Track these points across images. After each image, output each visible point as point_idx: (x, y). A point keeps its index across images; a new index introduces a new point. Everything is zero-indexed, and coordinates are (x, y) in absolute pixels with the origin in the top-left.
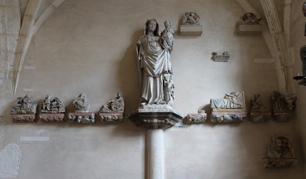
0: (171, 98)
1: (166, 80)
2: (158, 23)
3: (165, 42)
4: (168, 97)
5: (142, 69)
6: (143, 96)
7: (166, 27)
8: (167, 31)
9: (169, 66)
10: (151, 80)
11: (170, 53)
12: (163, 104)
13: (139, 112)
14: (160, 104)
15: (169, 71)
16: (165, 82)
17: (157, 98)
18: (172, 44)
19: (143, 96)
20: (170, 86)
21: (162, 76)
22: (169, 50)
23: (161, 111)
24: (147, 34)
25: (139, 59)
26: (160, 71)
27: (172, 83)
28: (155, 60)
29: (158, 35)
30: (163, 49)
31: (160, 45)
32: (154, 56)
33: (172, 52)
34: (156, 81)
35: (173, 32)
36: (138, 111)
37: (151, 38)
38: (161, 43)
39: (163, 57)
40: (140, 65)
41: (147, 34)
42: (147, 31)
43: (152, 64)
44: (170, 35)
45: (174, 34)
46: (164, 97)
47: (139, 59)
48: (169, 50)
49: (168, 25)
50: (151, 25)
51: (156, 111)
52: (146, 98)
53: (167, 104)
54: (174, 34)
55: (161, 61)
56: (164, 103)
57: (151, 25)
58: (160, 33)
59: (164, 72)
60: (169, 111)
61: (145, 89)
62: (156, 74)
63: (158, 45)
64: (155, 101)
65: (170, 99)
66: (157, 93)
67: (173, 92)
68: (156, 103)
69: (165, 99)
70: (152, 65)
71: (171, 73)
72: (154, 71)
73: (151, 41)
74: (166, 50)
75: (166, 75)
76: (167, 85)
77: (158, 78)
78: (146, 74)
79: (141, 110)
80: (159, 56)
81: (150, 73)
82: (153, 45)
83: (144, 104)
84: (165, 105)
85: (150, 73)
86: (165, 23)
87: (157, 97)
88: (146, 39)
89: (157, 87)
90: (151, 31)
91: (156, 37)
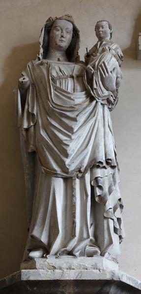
0: (115, 238)
1: (100, 187)
2: (78, 27)
3: (97, 79)
4: (106, 235)
5: (34, 156)
6: (36, 233)
7: (101, 39)
8: (104, 50)
9: (108, 145)
10: (59, 185)
11: (110, 109)
12: (91, 255)
13: (24, 278)
14: (83, 254)
15: (108, 161)
16: (98, 192)
17: (76, 238)
18: (117, 84)
19: (36, 233)
20: (110, 203)
21: (88, 176)
22: (109, 101)
23: (83, 278)
24: (46, 55)
25: (25, 126)
26: (82, 162)
27: (117, 194)
28: (70, 129)
30: (92, 98)
31: (84, 89)
34: (73, 189)
35: (120, 53)
36: (20, 275)
37: (59, 67)
38: (86, 81)
39: (92, 121)
40: (27, 142)
41: (46, 55)
42: (49, 47)
44: (111, 62)
46: (95, 236)
47: (25, 126)
48: (109, 101)
49: (105, 33)
50: (58, 33)
51: (71, 276)
52: (44, 239)
53: (102, 255)
54: (121, 58)
55: (85, 135)
56: (95, 253)
57: (58, 33)
58: (82, 54)
59: (94, 165)
60: (108, 277)
61: (41, 211)
62: (72, 168)
63: (78, 88)
64: (69, 248)
65: (111, 242)
66: (74, 223)
67: (119, 220)
68: (70, 253)
69: (97, 241)
70: (59, 143)
71: (113, 167)
72: (67, 161)
73: (60, 78)
74: (100, 102)
75: (99, 172)
76: (103, 200)
77: (77, 181)
78: (43, 169)
79: (28, 275)
80: (82, 119)
81: (54, 166)
83: (36, 254)
84: (96, 259)
85: (54, 166)
86: (97, 27)
87: (73, 236)
88: (45, 73)
89: (73, 206)
90: (59, 48)
91: (72, 65)
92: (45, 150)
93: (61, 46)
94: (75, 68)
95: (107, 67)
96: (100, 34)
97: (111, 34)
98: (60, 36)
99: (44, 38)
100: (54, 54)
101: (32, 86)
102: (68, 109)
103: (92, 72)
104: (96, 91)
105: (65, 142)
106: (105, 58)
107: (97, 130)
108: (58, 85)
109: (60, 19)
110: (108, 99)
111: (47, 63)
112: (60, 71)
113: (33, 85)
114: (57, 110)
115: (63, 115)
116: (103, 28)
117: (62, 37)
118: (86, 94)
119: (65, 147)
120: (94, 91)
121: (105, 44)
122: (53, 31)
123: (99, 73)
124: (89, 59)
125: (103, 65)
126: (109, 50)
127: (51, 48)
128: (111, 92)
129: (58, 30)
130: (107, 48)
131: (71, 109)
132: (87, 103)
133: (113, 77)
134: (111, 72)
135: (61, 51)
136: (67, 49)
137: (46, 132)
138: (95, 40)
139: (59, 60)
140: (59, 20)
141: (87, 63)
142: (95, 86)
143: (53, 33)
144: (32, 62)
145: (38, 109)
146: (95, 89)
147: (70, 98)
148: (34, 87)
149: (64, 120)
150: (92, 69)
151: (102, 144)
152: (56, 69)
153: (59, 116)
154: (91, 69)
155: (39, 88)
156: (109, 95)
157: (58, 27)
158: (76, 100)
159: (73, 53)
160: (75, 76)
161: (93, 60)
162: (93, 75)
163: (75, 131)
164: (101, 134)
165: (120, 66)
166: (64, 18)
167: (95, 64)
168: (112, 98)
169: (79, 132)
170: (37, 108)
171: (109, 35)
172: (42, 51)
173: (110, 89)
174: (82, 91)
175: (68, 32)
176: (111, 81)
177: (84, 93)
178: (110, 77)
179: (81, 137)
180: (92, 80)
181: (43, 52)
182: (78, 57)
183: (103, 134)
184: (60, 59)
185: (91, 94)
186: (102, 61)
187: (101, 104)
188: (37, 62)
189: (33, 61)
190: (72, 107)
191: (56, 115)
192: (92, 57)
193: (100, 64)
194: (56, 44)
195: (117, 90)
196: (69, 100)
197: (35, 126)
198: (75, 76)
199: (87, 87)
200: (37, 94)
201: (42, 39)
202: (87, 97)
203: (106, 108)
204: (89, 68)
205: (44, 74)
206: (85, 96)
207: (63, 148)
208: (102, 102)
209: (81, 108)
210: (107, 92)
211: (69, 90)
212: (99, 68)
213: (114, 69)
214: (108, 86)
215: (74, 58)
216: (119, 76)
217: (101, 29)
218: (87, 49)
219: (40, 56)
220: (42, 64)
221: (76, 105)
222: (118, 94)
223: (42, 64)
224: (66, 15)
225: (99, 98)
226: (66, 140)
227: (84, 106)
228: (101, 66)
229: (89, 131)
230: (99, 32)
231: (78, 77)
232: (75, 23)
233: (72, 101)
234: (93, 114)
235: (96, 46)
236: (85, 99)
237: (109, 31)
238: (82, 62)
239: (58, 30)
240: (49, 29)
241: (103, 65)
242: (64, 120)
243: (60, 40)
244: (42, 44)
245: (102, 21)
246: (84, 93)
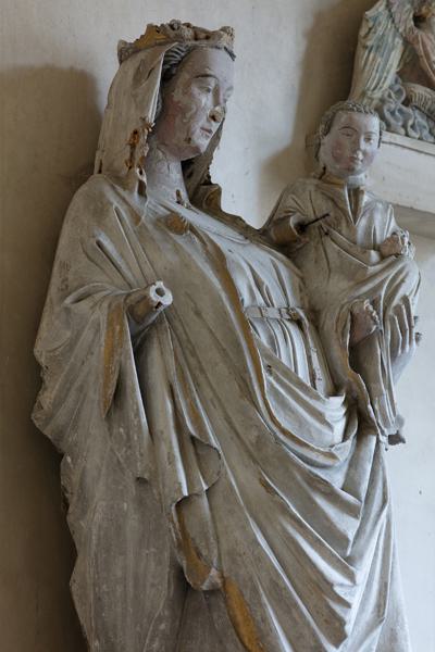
92: (265, 599)
105: (338, 590)
115: (321, 486)
119: (338, 609)
143: (187, 92)
149: (320, 501)
153: (305, 486)
157: (209, 79)
194: (189, 140)
196: (318, 425)
226: (342, 585)
228: (398, 310)
233: (325, 430)
242: (320, 501)
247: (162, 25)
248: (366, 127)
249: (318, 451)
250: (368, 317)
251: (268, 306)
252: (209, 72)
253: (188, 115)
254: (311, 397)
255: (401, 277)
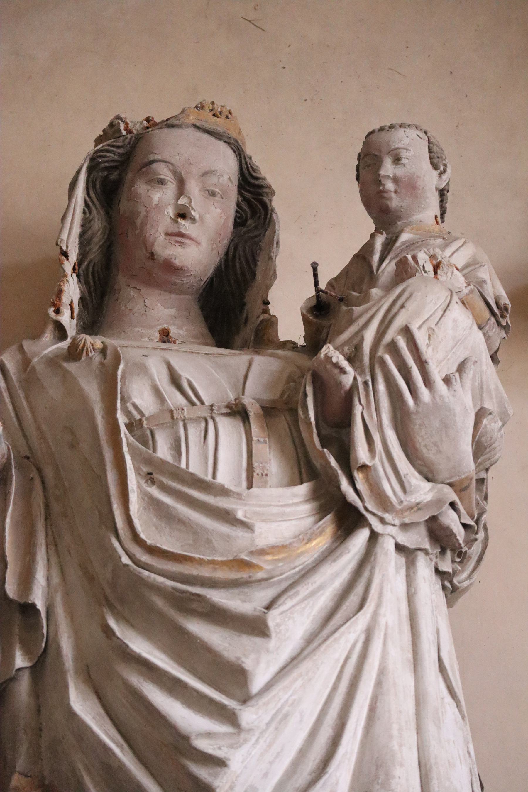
2: (268, 171)
7: (385, 217)
8: (404, 272)
18: (480, 448)
24: (96, 313)
28: (233, 677)
29: (263, 337)
30: (347, 519)
31: (304, 468)
32: (218, 616)
33: (481, 582)
35: (496, 290)
37: (166, 371)
38: (316, 435)
39: (351, 635)
41: (96, 313)
42: (113, 265)
43: (180, 744)
45: (497, 312)
49: (409, 186)
54: (497, 312)
58: (287, 306)
63: (272, 462)
74: (391, 535)
80: (292, 623)
82: (195, 466)
86: (369, 161)
88: (92, 390)
90: (163, 274)
91: (236, 360)
93: (177, 263)
94: (255, 368)
95: (427, 353)
96: (381, 194)
97: (442, 193)
98: (171, 212)
99: (86, 224)
100: (138, 307)
101: (19, 466)
102: (221, 574)
103: (347, 380)
104: (367, 479)
105: (203, 745)
106: (411, 306)
107: (379, 684)
108: (163, 451)
109: (169, 124)
110: (433, 519)
111: (103, 351)
112: (175, 381)
113: (28, 461)
114: (160, 579)
115: (194, 605)
116: (397, 160)
117: (183, 216)
118: (315, 495)
119: (202, 772)
120: (359, 477)
121: (410, 245)
122: (133, 182)
123: (381, 387)
124: (324, 323)
125: (402, 343)
126: (436, 268)
127: (121, 279)
128: (447, 490)
129: (162, 182)
130: (422, 257)
131: (233, 575)
132: (322, 542)
133: (458, 409)
134: (447, 380)
135: (181, 292)
136: (211, 281)
137: (99, 698)
138: (361, 227)
139: (165, 336)
140: (166, 131)
141: (315, 341)
142: (362, 453)
143: (134, 197)
144: (21, 349)
145: (56, 580)
146: (364, 467)
147: (227, 517)
148: (34, 474)
149: (197, 627)
150: (345, 364)
151: (410, 757)
152: (154, 371)
154: (336, 365)
155: (57, 471)
156: (438, 502)
157: (154, 166)
158: (260, 527)
159: (243, 305)
160: (253, 409)
161: (351, 322)
162: (348, 399)
163: (257, 684)
164: (400, 704)
165: (494, 358)
166: (192, 119)
167: (362, 339)
168: (452, 513)
169: (281, 694)
170: (48, 579)
171: (434, 200)
172: (72, 290)
173: (444, 475)
174: (292, 483)
175: (212, 194)
176: (446, 426)
177: (303, 489)
178: (438, 407)
179: (293, 721)
180: (345, 422)
181: (82, 300)
182: (270, 324)
183: (410, 706)
184: (174, 331)
185: (343, 497)
186: (399, 322)
187: (399, 548)
188: (48, 346)
189: (27, 345)
190: (241, 564)
191: (151, 608)
192: (344, 308)
193: (388, 338)
194: (152, 256)
195: (481, 481)
196: (223, 528)
197: (38, 669)
198: (253, 409)
199: (318, 464)
200: (47, 506)
201: (77, 230)
202: (322, 512)
203: (424, 569)
204: (328, 359)
205: (84, 399)
206: (307, 508)
207: (196, 780)
208: (404, 539)
209: (290, 570)
210: (427, 486)
211: (223, 478)
212: (383, 363)
213: (461, 368)
214: (429, 454)
215: (248, 332)
216: (488, 405)
217: (388, 168)
218: (315, 267)
219: (65, 318)
220: (74, 353)
221: (262, 552)
222: (490, 506)
223: (74, 353)
224: (201, 107)
225: (388, 517)
226: (209, 735)
227: (307, 559)
228: (393, 348)
229: (335, 688)
230: (379, 182)
231: (269, 411)
232: (249, 150)
233: (238, 533)
234: (354, 599)
235: (363, 257)
236: (311, 520)
237: (430, 180)
238: (291, 345)
239: (162, 182)
240: (114, 176)
241: (402, 343)
242: (197, 627)
243: (167, 234)
244: (73, 256)
245: (391, 127)
246: (303, 489)
247: (104, 131)
248: (388, 144)
249: (212, 562)
250: (329, 366)
251: (193, 404)
252: (151, 157)
253: (138, 222)
254: (215, 496)
255: (400, 303)
